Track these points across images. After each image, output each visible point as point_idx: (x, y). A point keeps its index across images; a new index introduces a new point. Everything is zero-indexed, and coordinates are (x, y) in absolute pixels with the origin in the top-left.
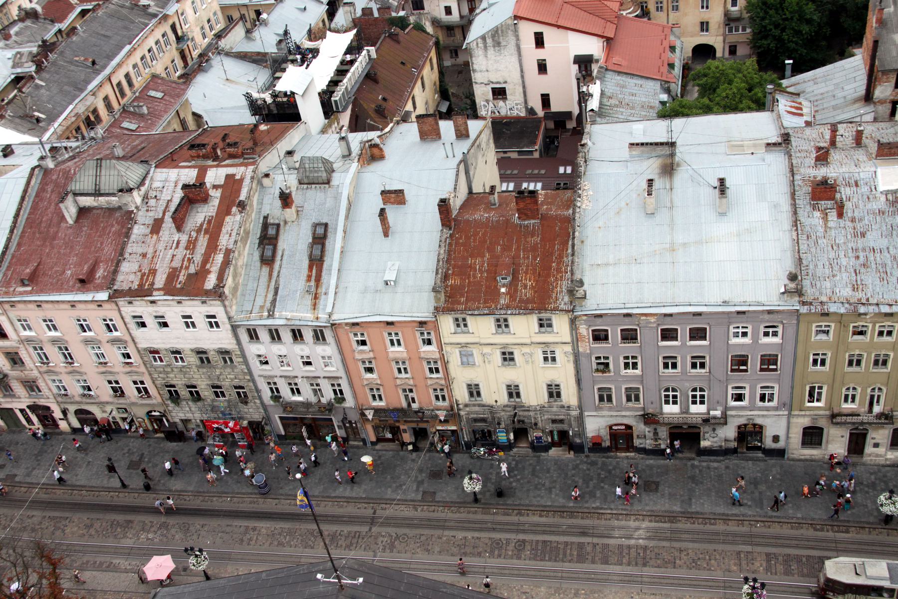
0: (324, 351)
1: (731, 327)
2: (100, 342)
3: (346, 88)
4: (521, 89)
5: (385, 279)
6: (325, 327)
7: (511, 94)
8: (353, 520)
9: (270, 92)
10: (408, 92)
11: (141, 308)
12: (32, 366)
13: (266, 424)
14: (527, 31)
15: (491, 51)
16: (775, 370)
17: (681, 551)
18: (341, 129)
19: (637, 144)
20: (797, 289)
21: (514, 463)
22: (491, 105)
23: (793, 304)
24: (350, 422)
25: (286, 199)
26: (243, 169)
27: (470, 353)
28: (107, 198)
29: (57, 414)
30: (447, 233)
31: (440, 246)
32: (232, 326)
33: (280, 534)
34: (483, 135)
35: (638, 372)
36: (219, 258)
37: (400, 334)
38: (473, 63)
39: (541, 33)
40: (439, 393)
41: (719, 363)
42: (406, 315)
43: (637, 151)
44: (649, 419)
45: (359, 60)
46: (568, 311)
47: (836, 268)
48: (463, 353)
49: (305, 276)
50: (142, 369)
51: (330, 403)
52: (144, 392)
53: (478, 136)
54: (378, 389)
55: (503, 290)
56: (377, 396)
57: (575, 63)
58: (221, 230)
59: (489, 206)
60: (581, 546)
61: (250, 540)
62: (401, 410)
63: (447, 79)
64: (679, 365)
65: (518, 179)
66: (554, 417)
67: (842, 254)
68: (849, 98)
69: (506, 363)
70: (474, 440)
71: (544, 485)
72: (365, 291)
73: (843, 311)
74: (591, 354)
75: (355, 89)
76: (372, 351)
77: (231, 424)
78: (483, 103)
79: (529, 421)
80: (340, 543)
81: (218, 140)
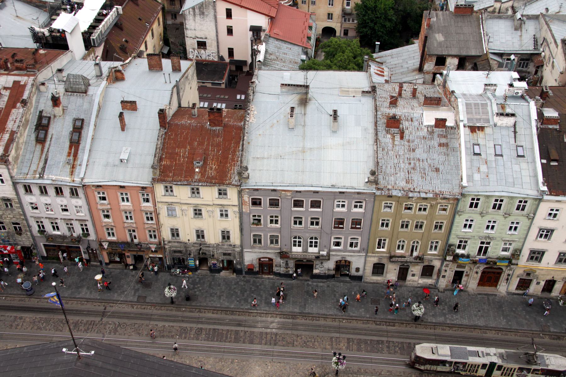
0: (77, 202)
1: (336, 201)
3: (101, 32)
4: (216, 44)
5: (121, 158)
6: (78, 187)
7: (209, 46)
8: (90, 313)
9: (48, 28)
10: (142, 38)
13: (34, 249)
14: (222, 7)
15: (198, 17)
16: (360, 228)
18: (96, 58)
19: (286, 85)
20: (375, 180)
21: (198, 279)
22: (196, 51)
23: (372, 189)
24: (92, 250)
25: (56, 101)
26: (26, 78)
27: (174, 209)
30: (163, 131)
31: (158, 139)
32: (13, 183)
33: (39, 322)
34: (189, 71)
35: (278, 226)
37: (129, 194)
38: (186, 24)
39: (231, 10)
40: (152, 233)
41: (327, 223)
42: (133, 182)
43: (285, 89)
44: (283, 255)
45: (111, 14)
47: (398, 169)
48: (169, 208)
49: (67, 152)
51: (79, 237)
53: (187, 71)
54: (112, 229)
55: (197, 170)
56: (111, 234)
57: (250, 30)
58: (8, 118)
59: (191, 116)
60: (237, 332)
61: (18, 325)
62: (127, 243)
63: (168, 33)
64: (303, 222)
65: (211, 100)
66: (224, 252)
67: (401, 162)
68: (410, 68)
69: (197, 216)
70: (173, 264)
71: (216, 294)
72: (107, 165)
73: (400, 195)
74: (250, 213)
75: (107, 33)
76: (109, 204)
77: (9, 248)
79: (209, 253)
80: (80, 328)
81: (9, 57)
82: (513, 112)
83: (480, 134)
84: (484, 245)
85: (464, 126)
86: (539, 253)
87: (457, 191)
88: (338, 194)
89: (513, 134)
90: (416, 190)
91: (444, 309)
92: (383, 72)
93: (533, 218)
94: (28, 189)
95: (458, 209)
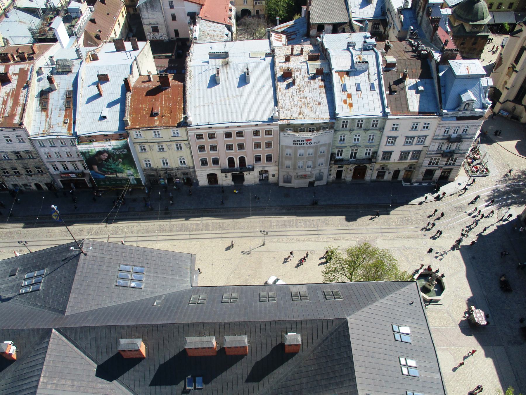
26: (28, 65)
36: (19, 109)
47: (293, 105)
53: (143, 49)
57: (188, 15)
78: (148, 34)
84: (354, 152)
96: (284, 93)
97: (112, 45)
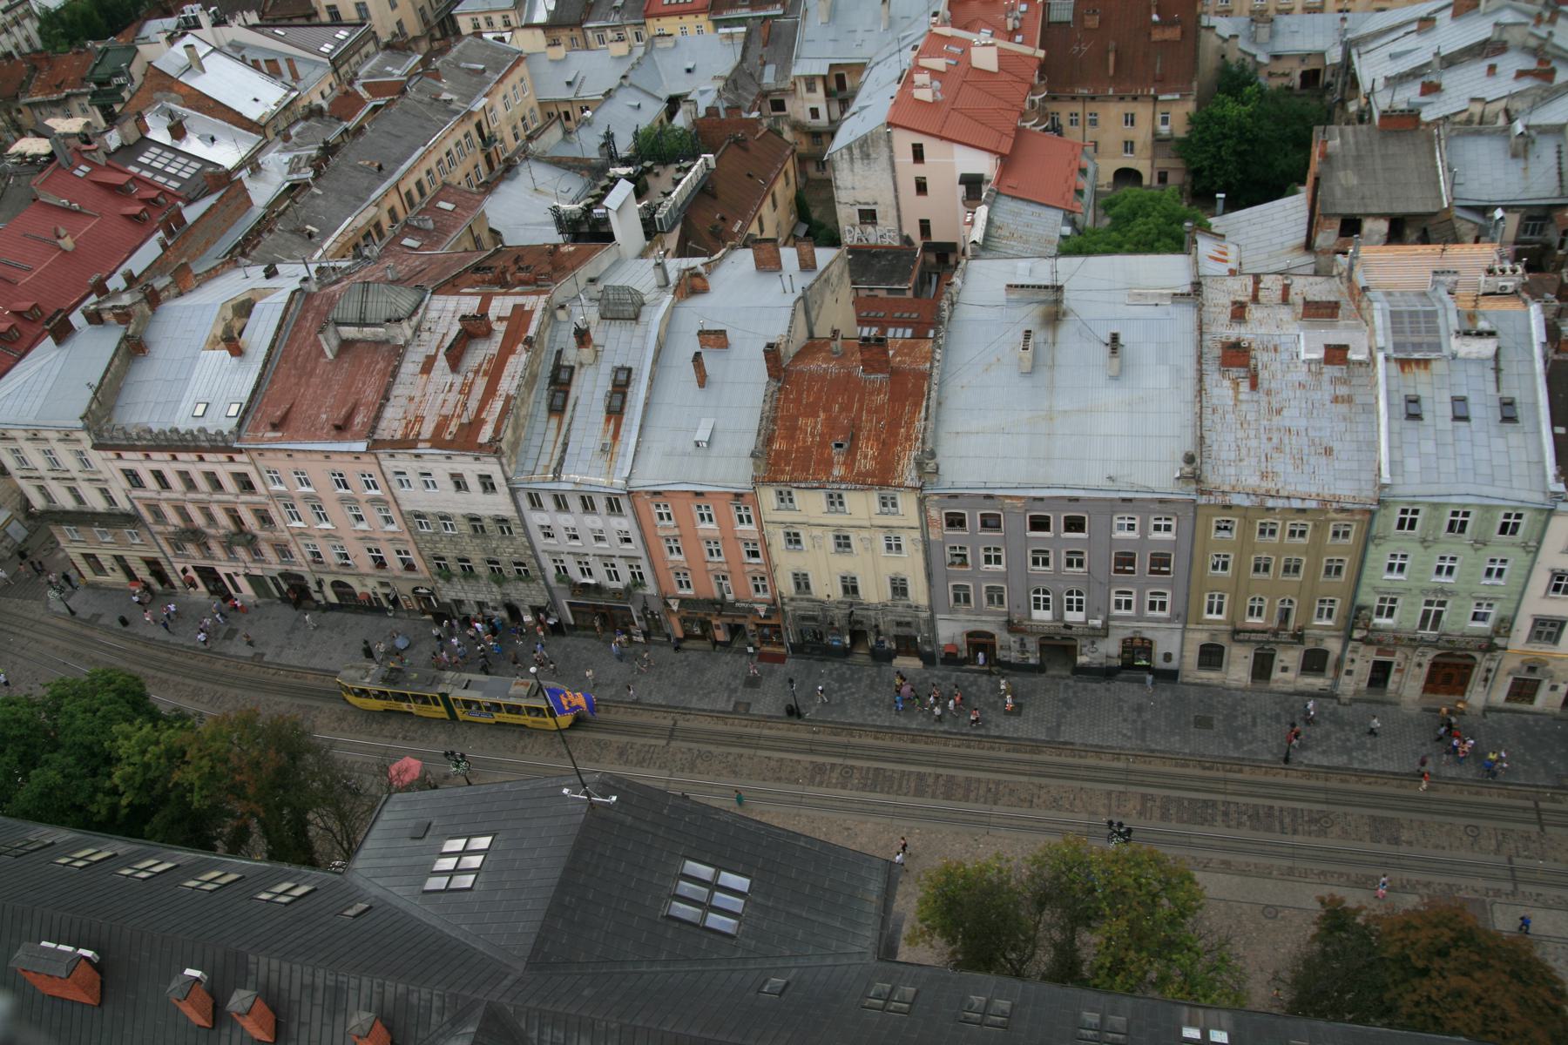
0: (620, 524)
1: (1115, 518)
2: (358, 501)
11: (403, 461)
12: (282, 526)
14: (904, 141)
15: (858, 165)
16: (1167, 573)
17: (1041, 787)
19: (1016, 286)
20: (1194, 473)
23: (1188, 492)
24: (652, 613)
26: (534, 298)
28: (373, 329)
29: (313, 586)
32: (510, 489)
35: (1001, 567)
36: (498, 405)
39: (921, 145)
41: (1099, 562)
43: (1015, 295)
44: (1011, 626)
46: (914, 488)
47: (1244, 452)
50: (407, 536)
52: (410, 567)
53: (827, 268)
57: (961, 183)
60: (921, 777)
61: (525, 747)
62: (713, 602)
64: (1051, 561)
66: (898, 619)
67: (1252, 434)
68: (1286, 244)
71: (883, 701)
73: (1246, 502)
74: (944, 544)
78: (847, 228)
82: (1494, 329)
83: (1421, 375)
84: (1434, 608)
85: (1387, 359)
86: (1552, 625)
87: (1368, 493)
88: (1120, 503)
89: (1491, 375)
90: (1282, 493)
91: (1349, 740)
92: (1225, 254)
93: (1538, 549)
94: (535, 502)
95: (1374, 532)
96: (1221, 411)
97: (745, 257)
